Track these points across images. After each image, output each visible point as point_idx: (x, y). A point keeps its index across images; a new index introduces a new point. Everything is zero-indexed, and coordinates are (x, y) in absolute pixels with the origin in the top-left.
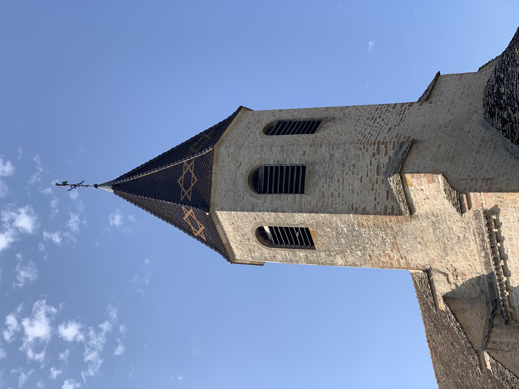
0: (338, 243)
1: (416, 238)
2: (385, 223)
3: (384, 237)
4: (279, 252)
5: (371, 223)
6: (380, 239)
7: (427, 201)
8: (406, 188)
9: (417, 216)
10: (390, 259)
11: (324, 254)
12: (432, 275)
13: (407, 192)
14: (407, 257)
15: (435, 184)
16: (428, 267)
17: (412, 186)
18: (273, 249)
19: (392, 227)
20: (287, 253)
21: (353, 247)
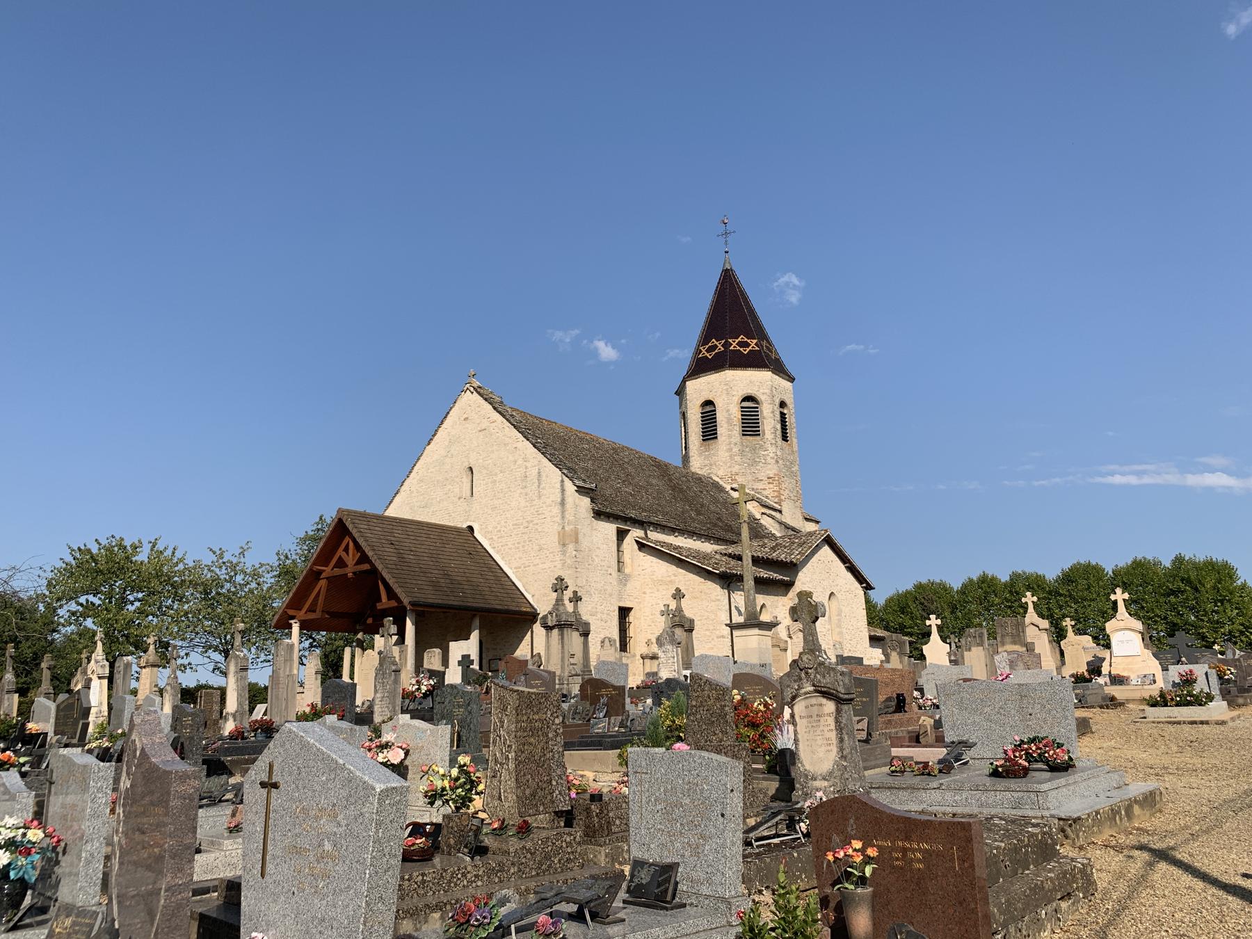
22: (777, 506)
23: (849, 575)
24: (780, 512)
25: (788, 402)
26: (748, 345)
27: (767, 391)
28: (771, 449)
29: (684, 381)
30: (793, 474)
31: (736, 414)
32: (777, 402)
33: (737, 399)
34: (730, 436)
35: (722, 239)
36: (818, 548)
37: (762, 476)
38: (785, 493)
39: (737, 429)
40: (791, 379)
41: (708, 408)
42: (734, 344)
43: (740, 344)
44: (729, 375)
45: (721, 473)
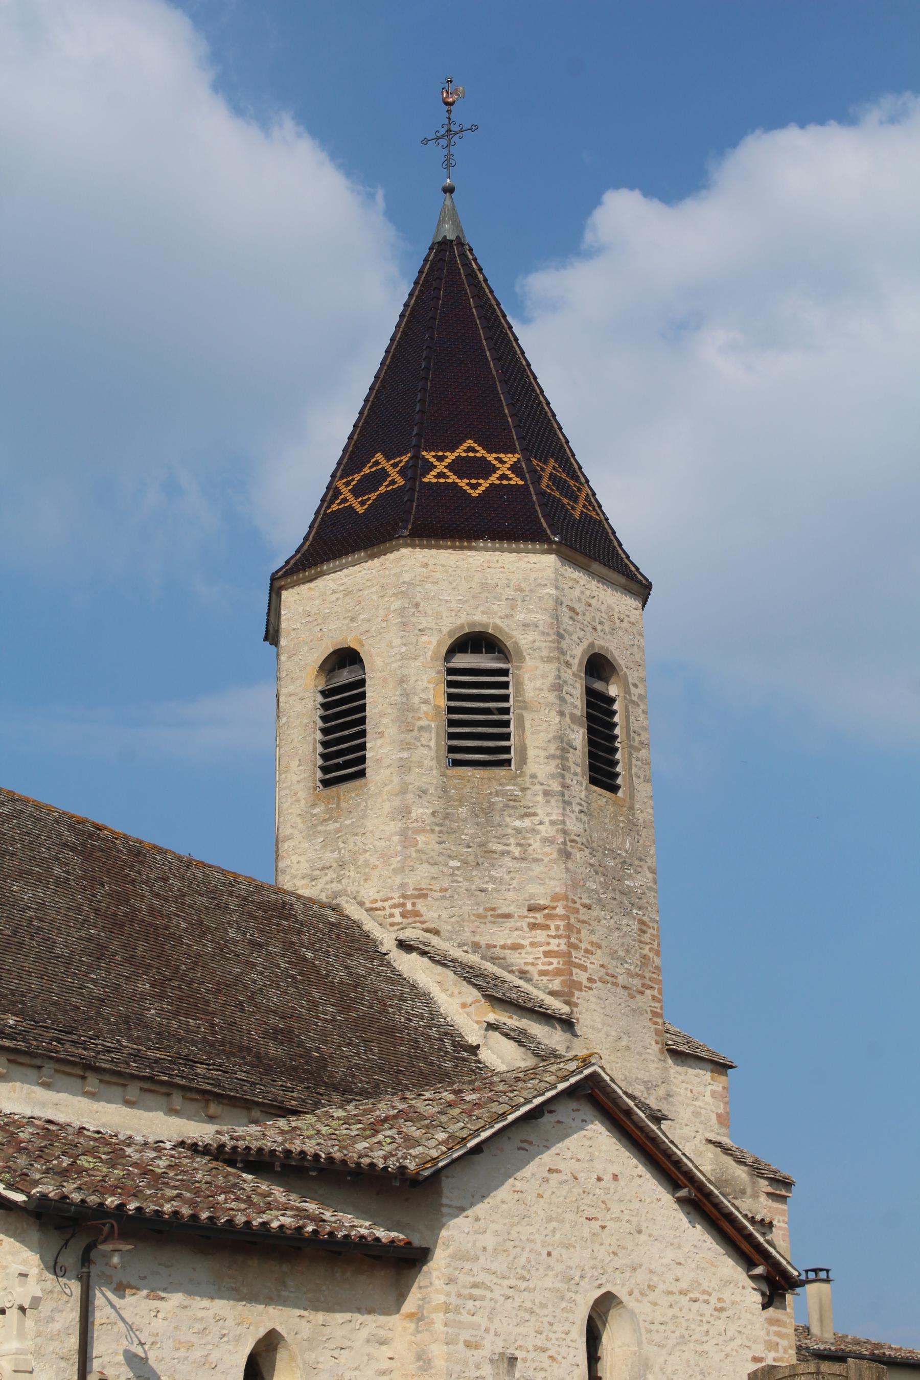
0: (605, 849)
1: (627, 1033)
2: (650, 983)
3: (626, 966)
4: (578, 685)
5: (646, 951)
6: (621, 953)
7: (689, 1095)
8: (710, 1066)
9: (664, 1061)
10: (587, 951)
11: (583, 795)
12: (563, 1030)
13: (703, 1064)
14: (591, 992)
15: (716, 1126)
16: (578, 1029)
17: (712, 1079)
18: (583, 675)
19: (642, 993)
20: (579, 703)
21: (602, 879)
22: (557, 1006)
23: (698, 1239)
24: (568, 1024)
25: (620, 658)
26: (485, 469)
27: (542, 618)
28: (547, 814)
29: (275, 592)
30: (628, 901)
31: (429, 690)
32: (577, 654)
33: (434, 642)
34: (404, 767)
35: (437, 152)
36: (530, 1128)
37: (509, 901)
38: (594, 963)
39: (431, 743)
40: (641, 588)
41: (345, 676)
42: (440, 468)
43: (461, 467)
44: (411, 565)
45: (369, 893)
